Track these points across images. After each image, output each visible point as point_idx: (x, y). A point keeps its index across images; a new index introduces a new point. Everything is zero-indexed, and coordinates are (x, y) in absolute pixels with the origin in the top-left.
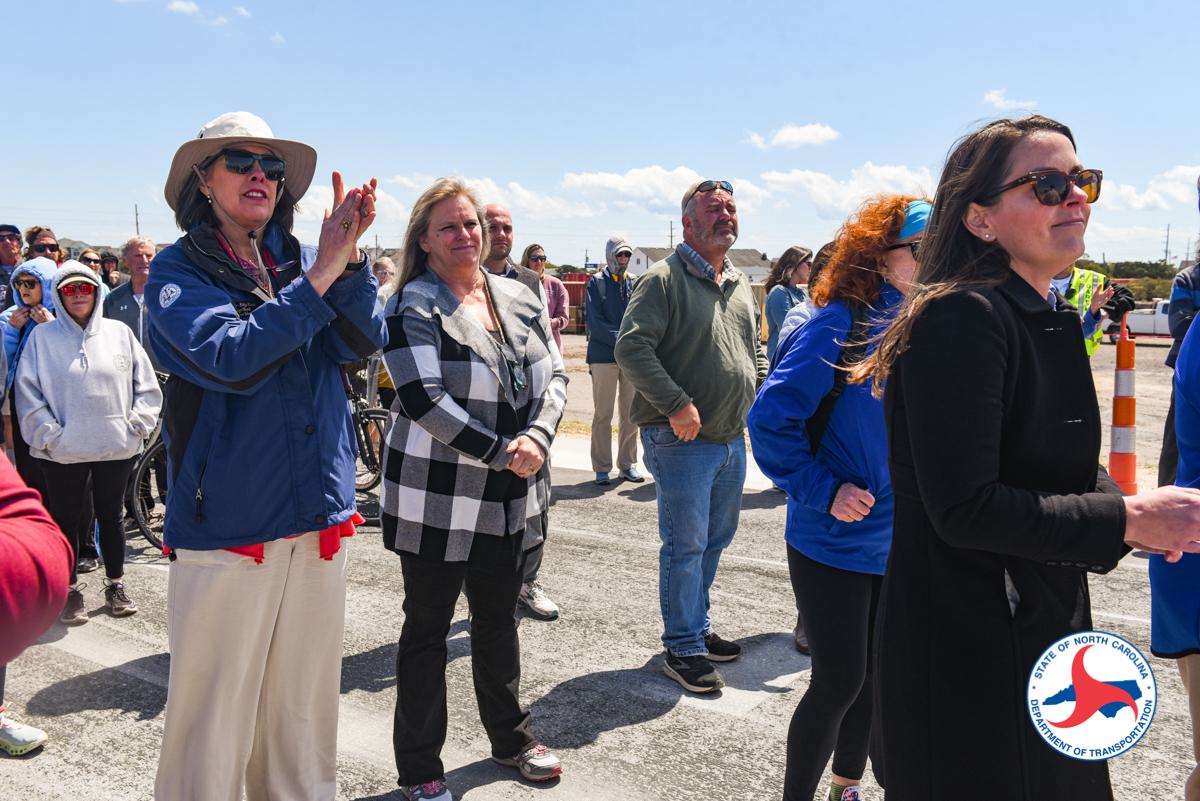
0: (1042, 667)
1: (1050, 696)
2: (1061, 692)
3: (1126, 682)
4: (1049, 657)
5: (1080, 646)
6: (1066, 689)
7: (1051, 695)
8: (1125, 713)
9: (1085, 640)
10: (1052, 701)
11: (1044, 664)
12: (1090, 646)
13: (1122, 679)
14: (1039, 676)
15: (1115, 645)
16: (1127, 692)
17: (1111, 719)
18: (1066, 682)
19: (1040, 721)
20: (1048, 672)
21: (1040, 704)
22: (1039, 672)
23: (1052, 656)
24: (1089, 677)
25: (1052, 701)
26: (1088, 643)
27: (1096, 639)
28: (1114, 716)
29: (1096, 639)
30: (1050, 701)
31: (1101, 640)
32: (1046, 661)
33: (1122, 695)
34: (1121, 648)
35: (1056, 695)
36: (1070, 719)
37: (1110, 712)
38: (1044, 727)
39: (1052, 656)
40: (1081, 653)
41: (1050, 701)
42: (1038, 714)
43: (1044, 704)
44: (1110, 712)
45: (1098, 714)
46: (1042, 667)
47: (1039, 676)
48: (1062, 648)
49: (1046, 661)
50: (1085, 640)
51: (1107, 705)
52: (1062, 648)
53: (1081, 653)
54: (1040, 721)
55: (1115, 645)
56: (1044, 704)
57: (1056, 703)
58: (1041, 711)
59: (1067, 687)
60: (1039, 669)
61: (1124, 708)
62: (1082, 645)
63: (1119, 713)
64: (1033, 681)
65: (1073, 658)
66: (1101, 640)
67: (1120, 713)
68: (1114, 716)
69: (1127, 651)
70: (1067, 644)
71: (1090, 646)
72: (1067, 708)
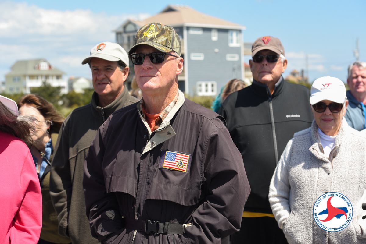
0: (318, 203)
1: (320, 212)
2: (324, 211)
3: (343, 208)
4: (320, 200)
5: (330, 197)
6: (325, 210)
7: (321, 212)
8: (343, 217)
9: (331, 195)
10: (321, 213)
11: (319, 202)
12: (332, 197)
13: (342, 207)
14: (317, 206)
15: (340, 196)
17: (339, 219)
18: (325, 208)
19: (317, 220)
20: (319, 205)
21: (317, 215)
22: (317, 205)
23: (321, 200)
24: (332, 206)
25: (321, 213)
26: (332, 196)
27: (334, 195)
28: (340, 218)
29: (334, 195)
30: (320, 214)
31: (336, 195)
32: (319, 201)
33: (342, 212)
35: (322, 212)
36: (326, 219)
37: (339, 217)
38: (318, 221)
39: (321, 200)
40: (330, 199)
41: (320, 214)
42: (317, 218)
43: (318, 214)
44: (339, 217)
45: (335, 217)
46: (318, 203)
47: (317, 206)
48: (324, 197)
49: (319, 201)
50: (331, 195)
51: (338, 215)
52: (324, 197)
53: (330, 199)
54: (317, 220)
55: (340, 196)
56: (318, 214)
57: (322, 214)
58: (317, 217)
59: (326, 209)
60: (317, 204)
61: (343, 216)
62: (330, 197)
63: (341, 217)
64: (315, 207)
65: (327, 200)
66: (336, 195)
67: (341, 217)
68: (340, 218)
70: (325, 196)
71: (332, 197)
72: (326, 216)
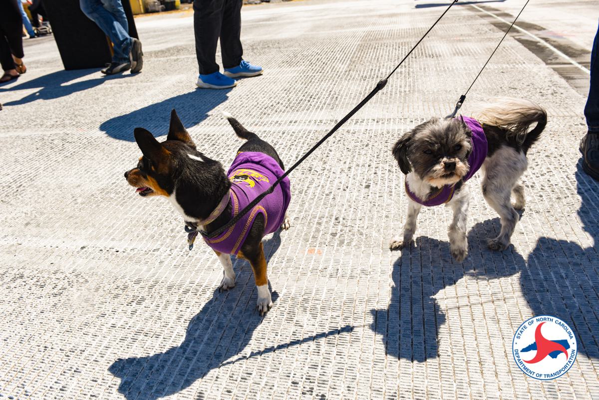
2: (529, 346)
3: (562, 341)
5: (539, 323)
7: (525, 347)
8: (562, 356)
10: (525, 350)
13: (560, 339)
16: (563, 345)
17: (554, 359)
18: (532, 340)
19: (519, 360)
21: (519, 352)
24: (544, 338)
25: (525, 350)
28: (556, 357)
30: (524, 350)
33: (560, 347)
34: (560, 324)
36: (534, 359)
37: (554, 355)
40: (540, 326)
41: (524, 350)
43: (521, 351)
44: (554, 355)
45: (548, 356)
51: (553, 352)
53: (540, 326)
56: (521, 351)
57: (527, 351)
62: (540, 322)
63: (559, 356)
67: (559, 356)
68: (556, 357)
69: (563, 325)
70: (532, 322)
72: (533, 354)
